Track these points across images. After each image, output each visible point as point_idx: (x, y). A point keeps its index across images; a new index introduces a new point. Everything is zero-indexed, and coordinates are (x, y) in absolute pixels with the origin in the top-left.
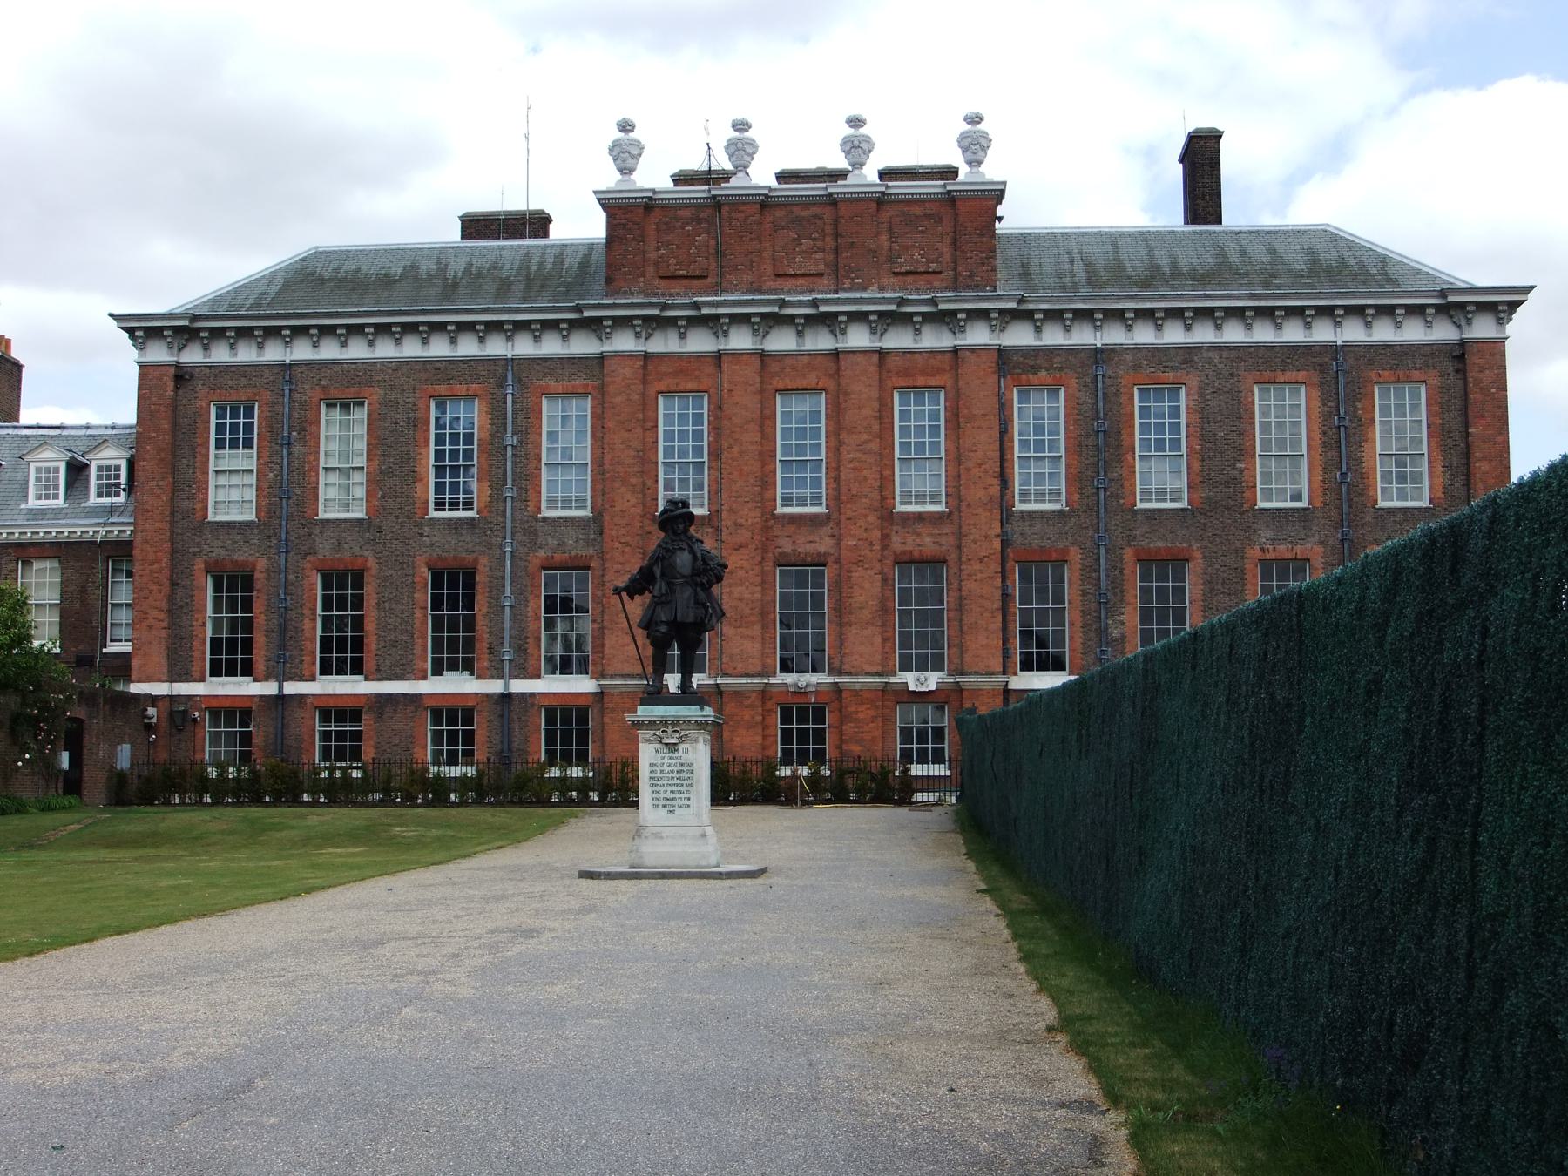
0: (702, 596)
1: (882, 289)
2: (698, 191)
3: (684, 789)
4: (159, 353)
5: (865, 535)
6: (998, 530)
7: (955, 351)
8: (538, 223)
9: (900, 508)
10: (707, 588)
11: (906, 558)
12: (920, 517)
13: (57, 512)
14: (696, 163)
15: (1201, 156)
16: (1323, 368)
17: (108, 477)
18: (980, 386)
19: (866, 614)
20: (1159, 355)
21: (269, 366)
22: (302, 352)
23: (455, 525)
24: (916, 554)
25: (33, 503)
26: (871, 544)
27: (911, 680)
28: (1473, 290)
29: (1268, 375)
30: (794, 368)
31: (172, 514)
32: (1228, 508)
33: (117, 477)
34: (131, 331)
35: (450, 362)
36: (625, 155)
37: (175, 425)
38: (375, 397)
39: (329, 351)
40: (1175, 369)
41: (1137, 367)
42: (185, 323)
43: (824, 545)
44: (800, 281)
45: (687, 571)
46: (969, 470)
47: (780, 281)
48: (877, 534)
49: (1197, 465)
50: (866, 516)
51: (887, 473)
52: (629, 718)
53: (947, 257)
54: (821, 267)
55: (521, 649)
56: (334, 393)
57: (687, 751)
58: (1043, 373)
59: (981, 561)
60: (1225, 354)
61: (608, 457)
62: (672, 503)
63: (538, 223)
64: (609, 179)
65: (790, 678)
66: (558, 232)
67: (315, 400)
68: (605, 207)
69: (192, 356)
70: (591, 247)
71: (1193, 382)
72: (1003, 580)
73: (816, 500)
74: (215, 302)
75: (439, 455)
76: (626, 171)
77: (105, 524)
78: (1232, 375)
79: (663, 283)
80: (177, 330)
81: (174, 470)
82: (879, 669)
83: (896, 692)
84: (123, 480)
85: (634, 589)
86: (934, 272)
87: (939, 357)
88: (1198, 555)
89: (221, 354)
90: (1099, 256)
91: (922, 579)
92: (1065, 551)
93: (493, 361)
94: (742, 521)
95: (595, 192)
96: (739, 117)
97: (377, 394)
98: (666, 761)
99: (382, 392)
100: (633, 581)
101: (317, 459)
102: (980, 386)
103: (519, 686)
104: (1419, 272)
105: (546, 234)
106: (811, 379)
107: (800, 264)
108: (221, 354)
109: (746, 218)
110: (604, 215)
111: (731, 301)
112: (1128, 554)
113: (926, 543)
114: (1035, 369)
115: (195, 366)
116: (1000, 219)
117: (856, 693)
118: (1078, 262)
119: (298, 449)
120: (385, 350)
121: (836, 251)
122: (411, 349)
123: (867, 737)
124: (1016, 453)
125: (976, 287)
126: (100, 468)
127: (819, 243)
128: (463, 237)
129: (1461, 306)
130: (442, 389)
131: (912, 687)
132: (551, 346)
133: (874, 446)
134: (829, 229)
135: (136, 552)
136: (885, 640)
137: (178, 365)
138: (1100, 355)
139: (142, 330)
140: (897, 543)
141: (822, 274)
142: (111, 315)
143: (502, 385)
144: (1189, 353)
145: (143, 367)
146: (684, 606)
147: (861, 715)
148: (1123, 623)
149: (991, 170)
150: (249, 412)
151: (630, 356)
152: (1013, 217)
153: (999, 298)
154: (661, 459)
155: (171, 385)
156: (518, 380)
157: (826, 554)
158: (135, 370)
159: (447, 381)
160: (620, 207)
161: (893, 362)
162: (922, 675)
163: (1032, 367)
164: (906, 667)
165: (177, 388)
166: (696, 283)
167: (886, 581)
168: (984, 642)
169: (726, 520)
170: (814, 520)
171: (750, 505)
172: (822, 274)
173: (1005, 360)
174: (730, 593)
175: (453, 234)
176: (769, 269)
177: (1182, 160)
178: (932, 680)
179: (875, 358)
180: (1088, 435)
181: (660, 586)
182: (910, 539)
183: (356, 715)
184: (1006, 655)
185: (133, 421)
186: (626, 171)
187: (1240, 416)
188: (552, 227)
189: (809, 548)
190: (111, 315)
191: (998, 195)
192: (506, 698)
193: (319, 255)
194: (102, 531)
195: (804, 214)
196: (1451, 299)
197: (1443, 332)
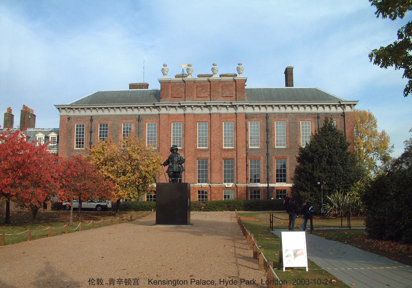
0: (180, 166)
1: (220, 100)
2: (180, 79)
4: (64, 113)
5: (216, 153)
6: (245, 152)
8: (147, 86)
9: (224, 147)
10: (181, 164)
11: (225, 158)
12: (228, 150)
14: (180, 73)
15: (288, 73)
16: (315, 118)
17: (53, 140)
18: (241, 121)
19: (216, 170)
20: (280, 115)
24: (227, 158)
26: (218, 155)
27: (226, 185)
28: (346, 101)
29: (303, 119)
30: (201, 117)
32: (295, 148)
33: (55, 140)
34: (58, 108)
40: (283, 118)
41: (275, 117)
42: (70, 107)
43: (208, 155)
44: (203, 98)
45: (177, 161)
46: (239, 139)
47: (198, 98)
48: (219, 153)
49: (288, 138)
50: (216, 149)
51: (221, 140)
53: (235, 94)
54: (207, 96)
58: (255, 118)
59: (242, 159)
60: (294, 115)
61: (160, 136)
62: (174, 146)
63: (147, 86)
65: (200, 184)
66: (150, 88)
68: (160, 82)
69: (71, 113)
71: (287, 120)
72: (246, 163)
73: (206, 146)
74: (77, 103)
78: (295, 119)
79: (173, 98)
80: (69, 108)
82: (219, 182)
83: (223, 187)
84: (56, 140)
85: (165, 165)
86: (231, 97)
87: (233, 115)
88: (288, 158)
89: (77, 113)
91: (228, 163)
92: (260, 157)
93: (135, 115)
94: (189, 150)
95: (158, 79)
99: (112, 122)
100: (165, 163)
102: (241, 121)
104: (335, 97)
105: (148, 88)
106: (205, 120)
107: (202, 95)
109: (191, 85)
110: (160, 84)
111: (188, 102)
112: (273, 157)
113: (229, 155)
114: (253, 118)
116: (246, 85)
117: (214, 187)
123: (217, 197)
124: (249, 136)
125: (241, 100)
126: (52, 138)
127: (207, 90)
128: (130, 89)
129: (344, 105)
130: (124, 121)
131: (226, 186)
132: (148, 112)
134: (209, 87)
136: (221, 176)
138: (267, 116)
139: (60, 108)
140: (223, 155)
141: (207, 97)
142: (55, 105)
144: (286, 114)
145: (61, 116)
146: (176, 167)
147: (215, 192)
148: (272, 173)
150: (83, 126)
151: (166, 114)
152: (249, 85)
153: (245, 102)
154: (172, 136)
155: (67, 120)
157: (208, 157)
158: (59, 117)
160: (163, 82)
161: (222, 116)
162: (229, 184)
163: (253, 117)
164: (225, 182)
166: (180, 98)
167: (221, 163)
168: (242, 176)
169: (186, 150)
170: (205, 150)
171: (192, 147)
172: (207, 97)
173: (247, 117)
174: (187, 166)
175: (127, 89)
176: (195, 95)
177: (285, 73)
178: (231, 185)
179: (219, 115)
180: (265, 132)
181: (170, 164)
182: (226, 154)
184: (247, 179)
187: (297, 127)
188: (149, 86)
189: (204, 156)
190: (55, 105)
191: (246, 81)
193: (98, 93)
195: (204, 84)
196: (341, 103)
197: (340, 110)
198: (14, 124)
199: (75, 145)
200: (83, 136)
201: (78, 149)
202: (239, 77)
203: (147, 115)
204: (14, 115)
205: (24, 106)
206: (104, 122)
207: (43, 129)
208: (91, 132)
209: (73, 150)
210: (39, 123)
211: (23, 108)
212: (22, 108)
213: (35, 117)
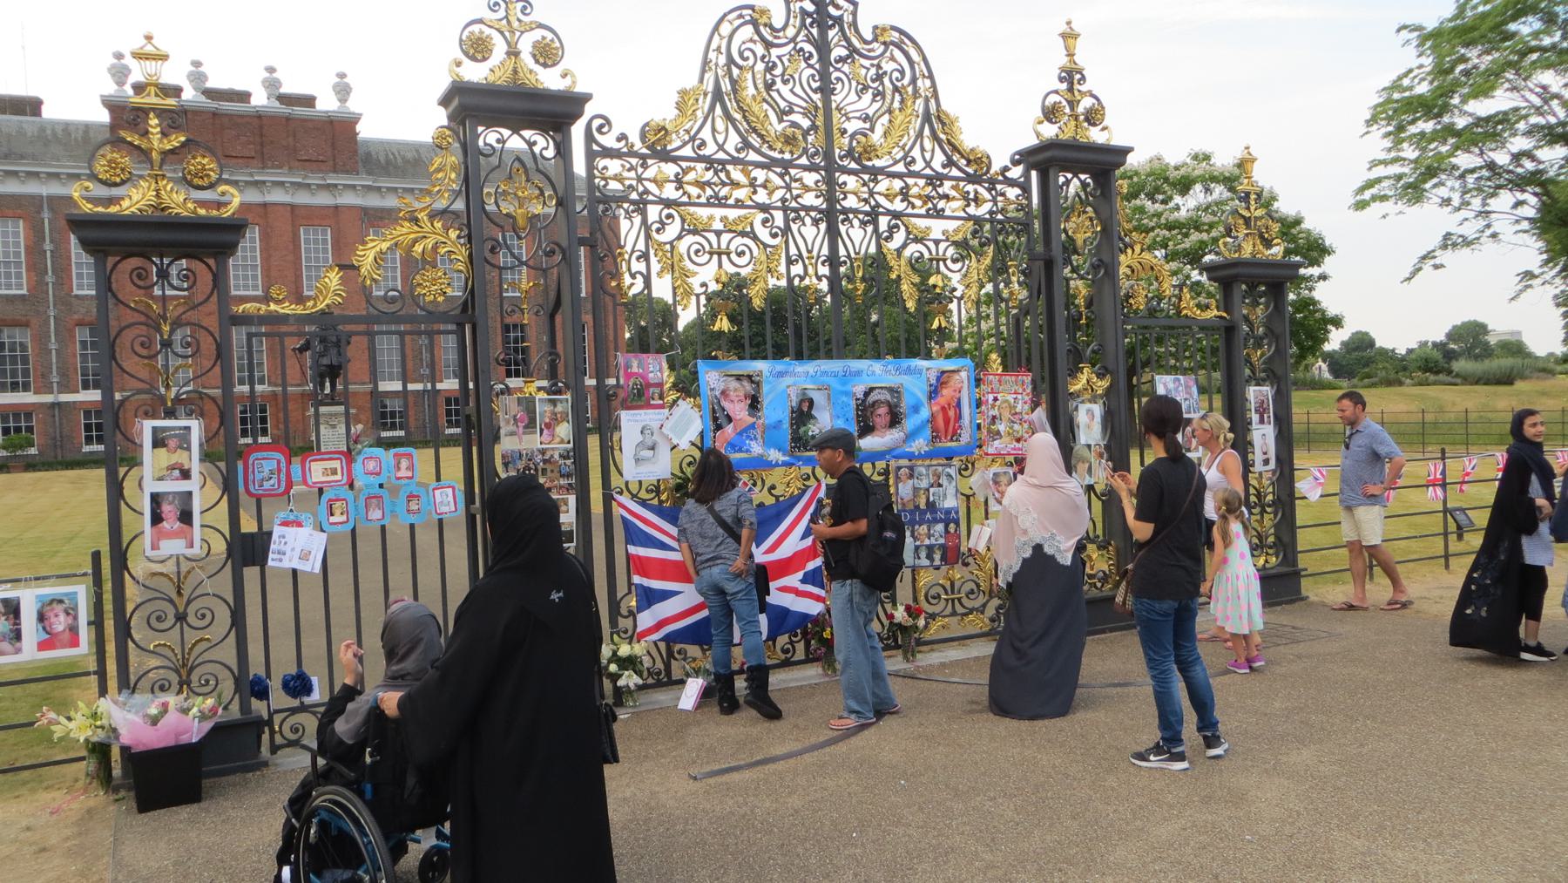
7: (336, 207)
36: (120, 74)
55: (63, 373)
64: (110, 88)
66: (48, 113)
70: (87, 127)
76: (121, 83)
90: (409, 155)
96: (196, 58)
103: (65, 398)
114: (382, 218)
118: (399, 160)
121: (262, 145)
125: (347, 172)
133: (291, 257)
143: (40, 210)
149: (353, 105)
152: (365, 131)
156: (51, 209)
183: (29, 416)
186: (121, 83)
192: (53, 405)
202: (327, 103)
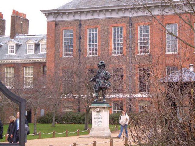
3: (101, 121)
4: (52, 19)
13: (33, 55)
21: (76, 21)
22: (83, 17)
23: (118, 58)
25: (28, 53)
31: (55, 56)
34: (45, 14)
35: (117, 18)
37: (55, 35)
38: (100, 27)
39: (89, 17)
42: (56, 12)
52: (90, 106)
56: (91, 26)
57: (101, 113)
67: (86, 29)
69: (59, 19)
74: (65, 6)
75: (114, 41)
77: (42, 58)
80: (55, 13)
81: (55, 46)
89: (65, 18)
93: (127, 17)
97: (100, 27)
98: (97, 115)
101: (87, 43)
108: (65, 18)
115: (60, 21)
119: (82, 40)
120: (102, 16)
122: (108, 16)
130: (115, 25)
135: (47, 65)
137: (56, 21)
139: (48, 14)
142: (41, 11)
145: (48, 22)
155: (54, 26)
158: (46, 22)
159: (116, 23)
165: (56, 26)
185: (46, 33)
190: (41, 11)
194: (42, 60)
198: (6, 30)
199: (64, 53)
200: (71, 43)
201: (67, 57)
203: (139, 17)
204: (5, 20)
205: (14, 11)
206: (94, 26)
207: (34, 35)
208: (80, 38)
209: (61, 59)
210: (32, 30)
211: (13, 13)
212: (11, 13)
213: (28, 22)
